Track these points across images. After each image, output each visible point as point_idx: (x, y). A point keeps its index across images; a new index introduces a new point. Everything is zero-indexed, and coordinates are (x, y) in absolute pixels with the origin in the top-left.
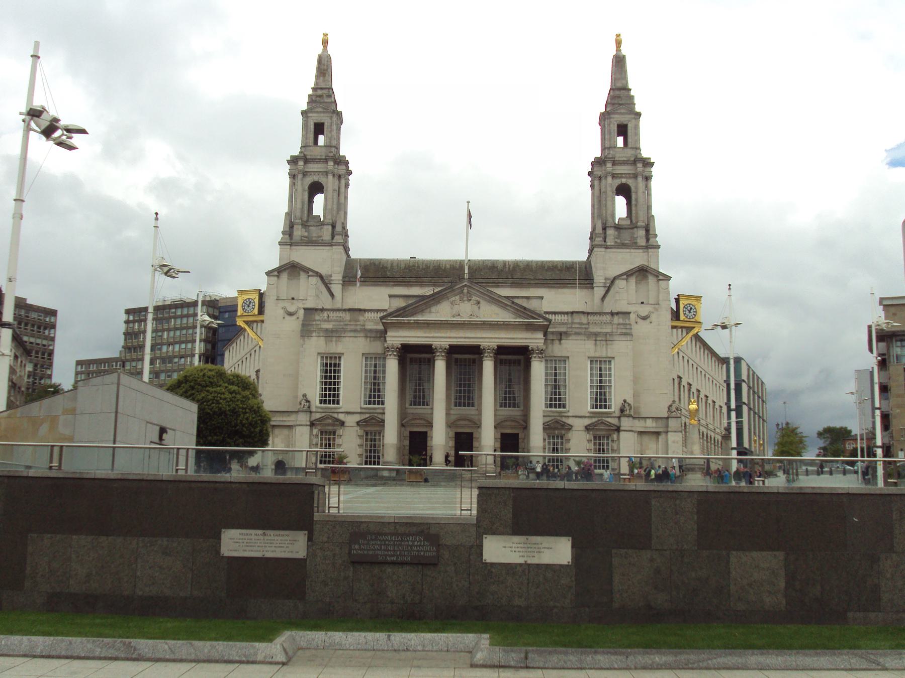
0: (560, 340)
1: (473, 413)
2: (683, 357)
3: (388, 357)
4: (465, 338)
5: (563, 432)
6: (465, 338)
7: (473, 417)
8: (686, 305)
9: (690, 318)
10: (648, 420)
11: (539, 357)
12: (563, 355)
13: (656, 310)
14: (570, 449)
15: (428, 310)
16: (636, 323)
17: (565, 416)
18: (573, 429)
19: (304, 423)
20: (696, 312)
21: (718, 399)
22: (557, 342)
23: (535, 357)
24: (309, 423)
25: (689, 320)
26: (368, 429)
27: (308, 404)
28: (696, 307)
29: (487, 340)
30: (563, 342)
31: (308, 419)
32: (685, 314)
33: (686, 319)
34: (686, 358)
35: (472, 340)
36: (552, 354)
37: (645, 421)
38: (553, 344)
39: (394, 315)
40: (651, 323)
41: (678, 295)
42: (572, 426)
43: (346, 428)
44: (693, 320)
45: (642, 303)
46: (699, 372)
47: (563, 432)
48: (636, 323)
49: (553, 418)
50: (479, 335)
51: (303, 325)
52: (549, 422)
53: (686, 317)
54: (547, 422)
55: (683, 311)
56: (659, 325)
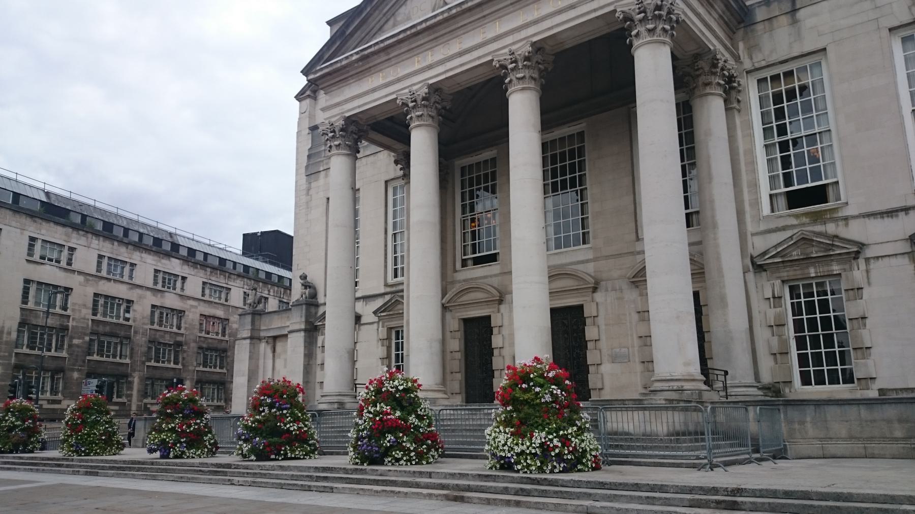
0: (794, 11)
1: (581, 257)
3: (334, 151)
4: (461, 54)
5: (836, 268)
6: (461, 54)
7: (580, 267)
11: (649, 31)
12: (808, 48)
14: (864, 318)
15: (391, 23)
17: (835, 220)
18: (869, 253)
19: (297, 327)
22: (784, 20)
23: (637, 35)
24: (303, 327)
26: (393, 324)
27: (307, 291)
29: (509, 40)
30: (801, 14)
31: (303, 319)
35: (476, 54)
36: (774, 58)
38: (772, 30)
39: (326, 56)
42: (862, 246)
43: (362, 327)
47: (836, 268)
49: (795, 231)
50: (490, 35)
51: (309, 157)
52: (779, 244)
54: (776, 247)
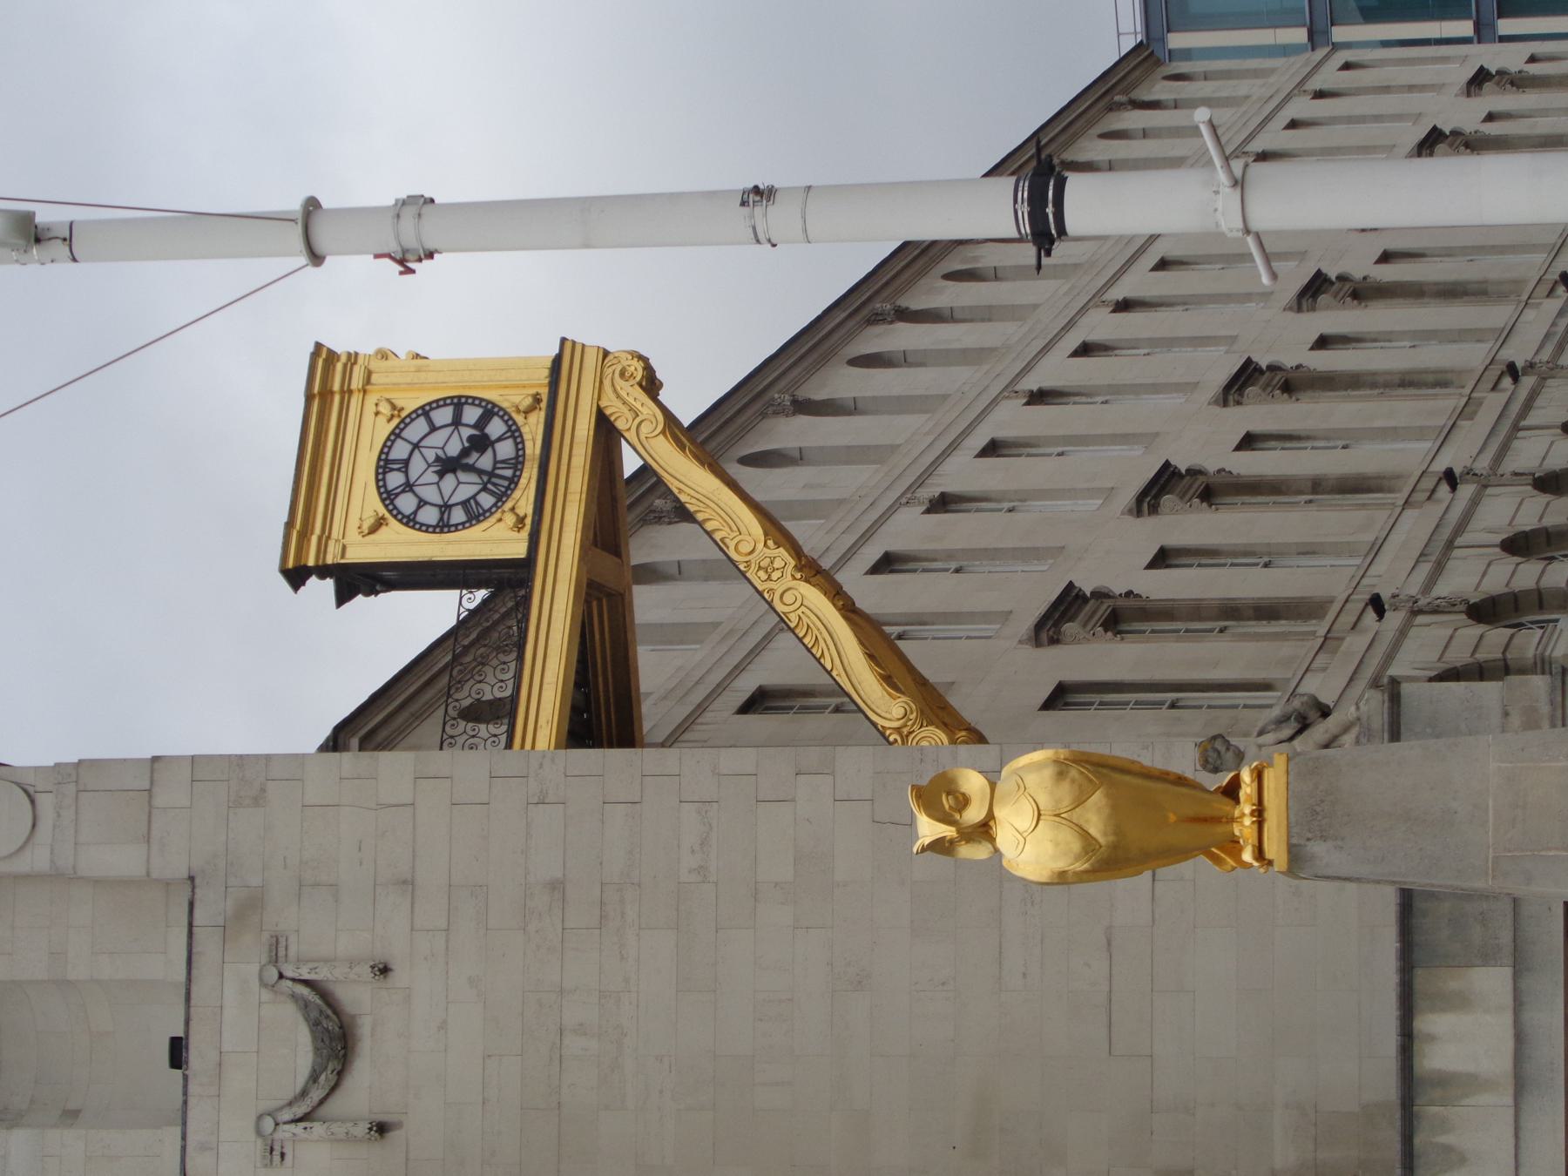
2: (993, 449)
8: (388, 497)
9: (518, 463)
10: (1434, 1059)
13: (251, 906)
16: (382, 1129)
20: (458, 403)
21: (1415, 102)
25: (530, 475)
28: (411, 402)
32: (475, 515)
33: (524, 499)
34: (1012, 420)
37: (1444, 1081)
40: (384, 970)
41: (296, 576)
44: (533, 428)
45: (178, 1052)
46: (1166, 285)
48: (382, 1129)
53: (501, 498)
55: (443, 526)
56: (408, 884)
